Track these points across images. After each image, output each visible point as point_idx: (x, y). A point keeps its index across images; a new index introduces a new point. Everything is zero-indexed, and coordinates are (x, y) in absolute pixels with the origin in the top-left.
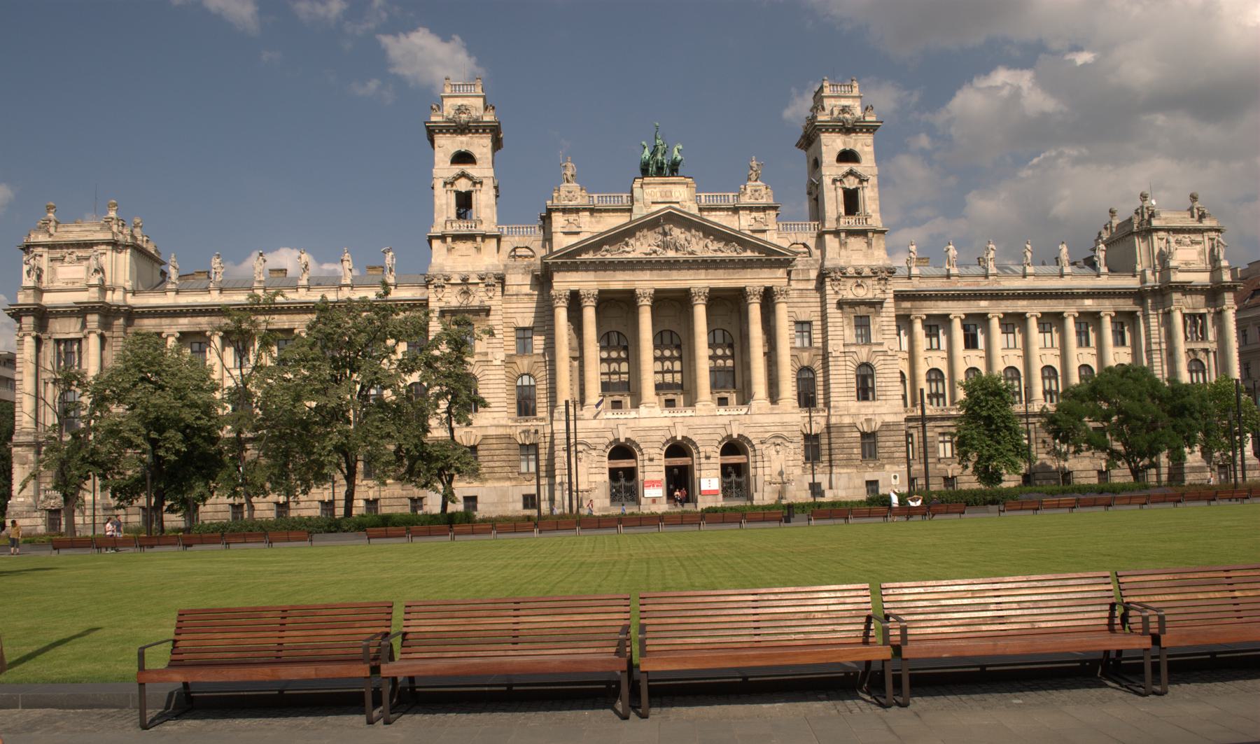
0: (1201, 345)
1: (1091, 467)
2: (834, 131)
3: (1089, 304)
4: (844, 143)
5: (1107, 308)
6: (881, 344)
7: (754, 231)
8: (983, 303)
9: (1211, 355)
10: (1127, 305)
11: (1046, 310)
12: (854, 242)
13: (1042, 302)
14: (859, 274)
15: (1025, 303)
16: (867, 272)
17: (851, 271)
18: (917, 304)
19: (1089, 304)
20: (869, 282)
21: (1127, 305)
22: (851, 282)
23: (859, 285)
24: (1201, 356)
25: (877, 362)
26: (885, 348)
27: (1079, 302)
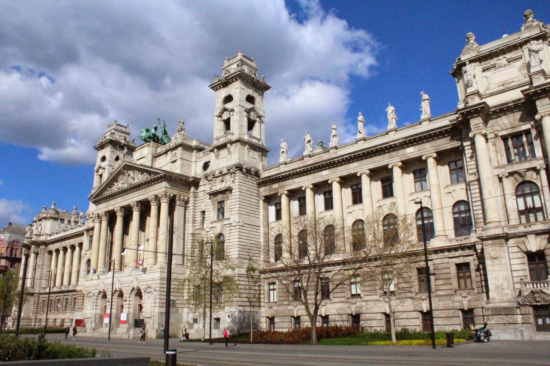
0: (527, 165)
1: (411, 308)
2: (220, 88)
3: (411, 152)
4: (226, 92)
5: (427, 150)
6: (229, 219)
7: (173, 162)
8: (325, 173)
9: (543, 173)
10: (445, 144)
11: (373, 166)
12: (224, 152)
13: (369, 160)
14: (222, 174)
15: (355, 164)
16: (225, 171)
17: (217, 173)
18: (282, 184)
19: (411, 152)
20: (227, 177)
21: (445, 144)
22: (218, 180)
23: (222, 181)
24: (531, 176)
25: (226, 233)
26: (231, 221)
27: (401, 152)
